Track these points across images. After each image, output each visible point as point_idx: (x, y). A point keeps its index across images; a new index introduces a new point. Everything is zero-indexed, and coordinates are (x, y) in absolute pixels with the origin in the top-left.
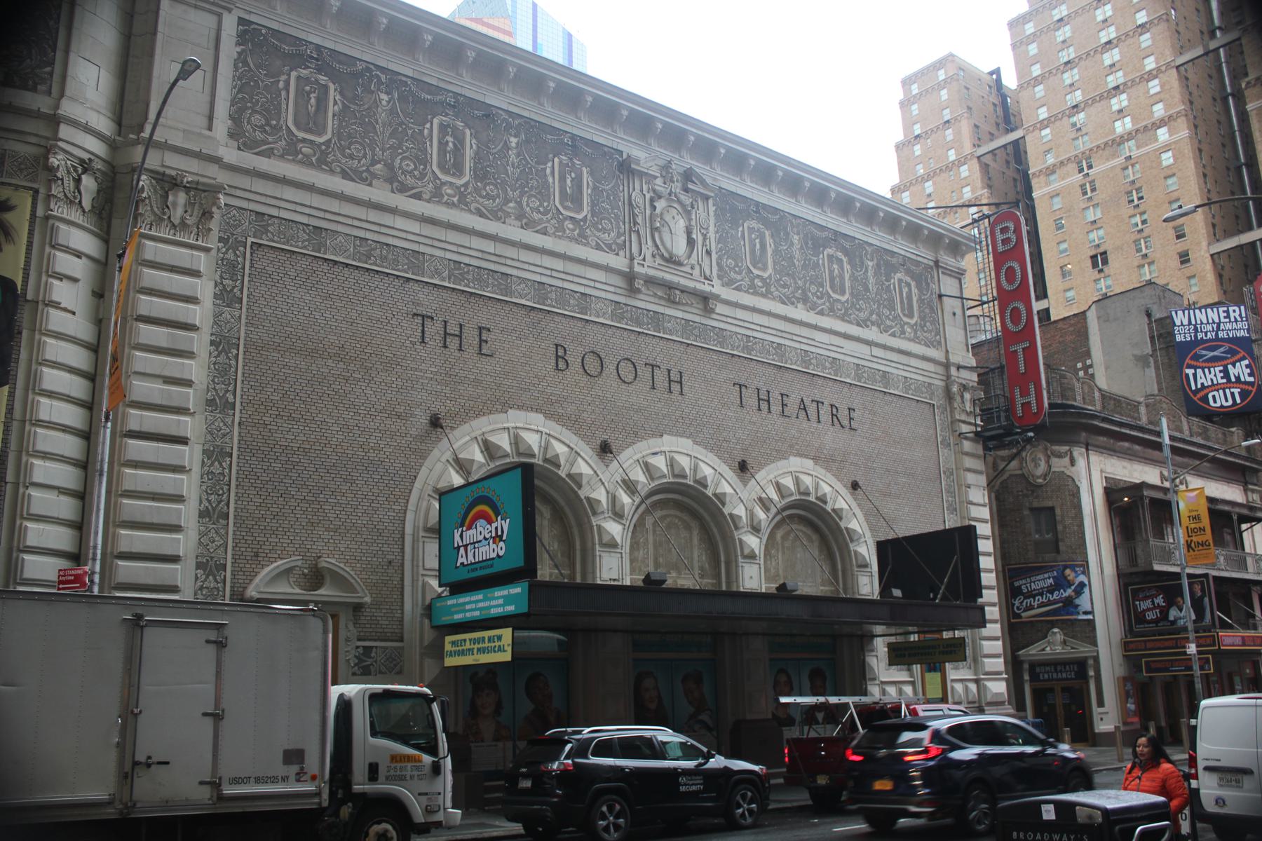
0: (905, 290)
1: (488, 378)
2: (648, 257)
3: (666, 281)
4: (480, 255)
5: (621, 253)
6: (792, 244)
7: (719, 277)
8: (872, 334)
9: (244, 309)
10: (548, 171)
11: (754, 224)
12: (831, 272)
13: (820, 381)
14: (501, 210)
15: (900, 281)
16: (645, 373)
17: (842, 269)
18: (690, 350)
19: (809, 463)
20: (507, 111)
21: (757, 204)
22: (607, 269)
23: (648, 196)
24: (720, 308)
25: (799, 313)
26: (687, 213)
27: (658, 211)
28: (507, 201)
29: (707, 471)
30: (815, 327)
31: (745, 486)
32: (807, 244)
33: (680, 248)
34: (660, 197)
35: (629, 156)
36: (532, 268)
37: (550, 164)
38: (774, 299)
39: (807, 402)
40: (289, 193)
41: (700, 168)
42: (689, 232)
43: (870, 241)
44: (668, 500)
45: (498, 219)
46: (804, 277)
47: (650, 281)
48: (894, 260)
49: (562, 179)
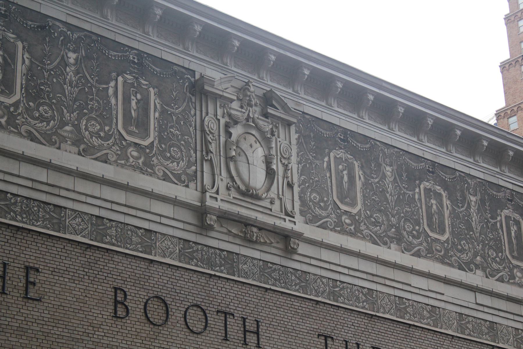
0: (514, 229)
1: (35, 327)
2: (223, 190)
3: (241, 217)
4: (29, 184)
5: (192, 185)
6: (384, 176)
7: (302, 213)
10: (111, 91)
11: (341, 154)
12: (429, 208)
13: (418, 333)
14: (56, 133)
15: (507, 218)
16: (216, 322)
17: (442, 207)
20: (65, 23)
21: (345, 131)
22: (175, 202)
23: (222, 121)
24: (303, 248)
25: (392, 254)
26: (266, 140)
27: (234, 138)
28: (63, 124)
30: (411, 271)
32: (401, 176)
33: (258, 179)
34: (236, 123)
35: (202, 76)
36: (90, 200)
37: (112, 84)
38: (364, 238)
41: (281, 90)
42: (268, 162)
43: (473, 173)
45: (52, 144)
46: (398, 213)
48: (501, 195)
49: (127, 101)
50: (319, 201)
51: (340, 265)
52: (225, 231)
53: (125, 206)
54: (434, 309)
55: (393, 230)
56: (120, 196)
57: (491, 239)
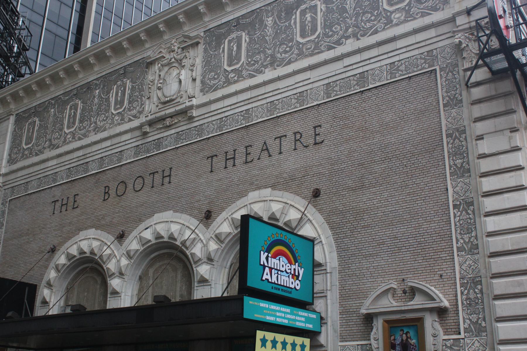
8: (350, 45)
9: (4, 227)
13: (285, 119)
16: (148, 180)
18: (179, 151)
19: (267, 192)
22: (131, 130)
24: (195, 113)
25: (269, 74)
29: (175, 228)
31: (208, 228)
39: (270, 142)
40: (20, 174)
44: (164, 254)
47: (151, 123)
50: (215, 75)
51: (224, 107)
52: (155, 129)
53: (111, 146)
54: (302, 94)
55: (269, 59)
56: (108, 143)
57: (366, 6)
